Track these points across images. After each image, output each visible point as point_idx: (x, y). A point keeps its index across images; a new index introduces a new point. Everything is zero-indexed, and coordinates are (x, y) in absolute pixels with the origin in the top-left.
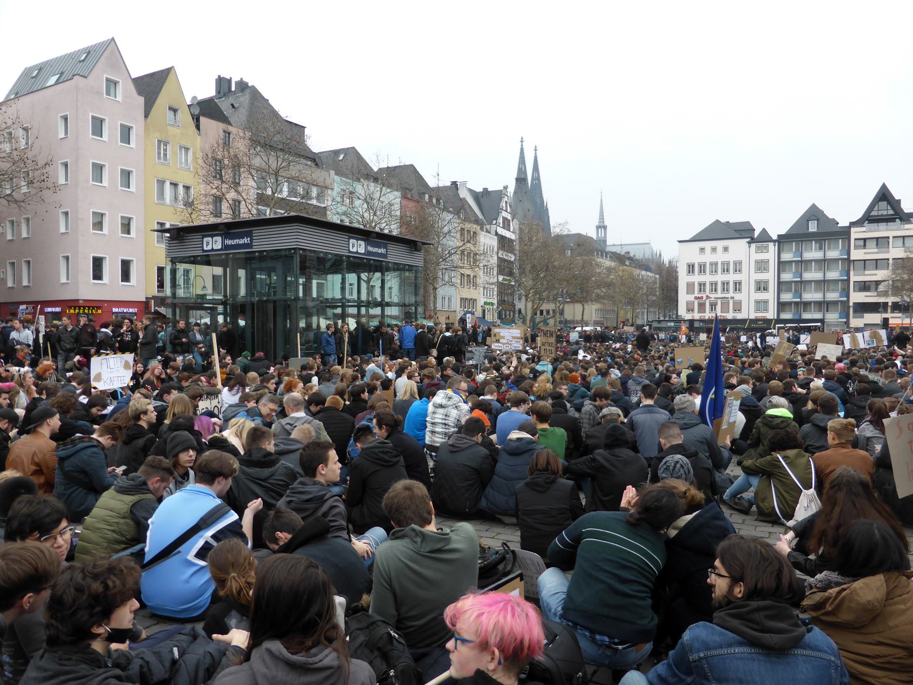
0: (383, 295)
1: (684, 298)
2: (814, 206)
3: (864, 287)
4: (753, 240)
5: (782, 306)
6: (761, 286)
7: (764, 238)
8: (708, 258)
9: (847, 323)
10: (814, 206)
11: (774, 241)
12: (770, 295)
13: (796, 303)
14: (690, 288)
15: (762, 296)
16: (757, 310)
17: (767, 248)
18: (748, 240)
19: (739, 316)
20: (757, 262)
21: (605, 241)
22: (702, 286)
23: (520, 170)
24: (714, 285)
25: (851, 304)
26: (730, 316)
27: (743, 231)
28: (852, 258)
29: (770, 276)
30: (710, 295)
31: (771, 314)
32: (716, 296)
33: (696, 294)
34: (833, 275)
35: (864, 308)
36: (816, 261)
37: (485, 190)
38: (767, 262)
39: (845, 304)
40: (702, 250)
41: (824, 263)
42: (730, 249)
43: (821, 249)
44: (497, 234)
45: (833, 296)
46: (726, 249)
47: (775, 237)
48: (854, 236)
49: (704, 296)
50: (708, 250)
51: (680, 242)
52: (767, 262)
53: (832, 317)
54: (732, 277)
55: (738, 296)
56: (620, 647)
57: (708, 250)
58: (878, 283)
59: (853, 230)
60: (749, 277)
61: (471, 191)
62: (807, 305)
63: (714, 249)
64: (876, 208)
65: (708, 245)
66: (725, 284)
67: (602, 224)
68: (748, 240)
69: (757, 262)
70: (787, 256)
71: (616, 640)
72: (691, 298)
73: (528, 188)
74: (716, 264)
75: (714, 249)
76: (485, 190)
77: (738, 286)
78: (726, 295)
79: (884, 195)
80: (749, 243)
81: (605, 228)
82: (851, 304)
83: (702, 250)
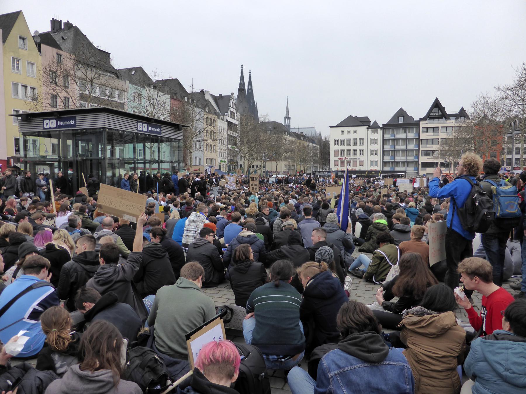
0: (159, 157)
1: (333, 159)
2: (401, 109)
3: (427, 153)
4: (369, 127)
5: (385, 163)
7: (375, 126)
8: (346, 136)
9: (418, 173)
10: (401, 109)
11: (381, 128)
12: (378, 158)
13: (392, 162)
14: (336, 152)
15: (374, 158)
16: (372, 166)
17: (377, 131)
19: (362, 169)
20: (372, 139)
21: (289, 126)
22: (343, 152)
23: (241, 84)
24: (349, 151)
25: (420, 163)
26: (357, 169)
27: (364, 122)
29: (378, 147)
31: (379, 168)
32: (350, 158)
34: (411, 147)
35: (426, 165)
36: (402, 139)
37: (220, 95)
38: (377, 139)
39: (417, 163)
40: (343, 132)
41: (406, 140)
42: (357, 132)
43: (405, 132)
44: (227, 121)
45: (411, 158)
46: (355, 132)
47: (381, 126)
50: (346, 132)
51: (331, 127)
52: (377, 139)
54: (358, 147)
55: (361, 158)
56: (283, 360)
57: (346, 132)
58: (433, 152)
59: (421, 122)
60: (367, 147)
61: (212, 96)
62: (397, 163)
63: (349, 132)
64: (433, 111)
65: (346, 129)
66: (355, 151)
67: (287, 116)
69: (372, 139)
70: (387, 136)
71: (281, 356)
72: (337, 158)
73: (246, 94)
74: (350, 140)
75: (349, 132)
76: (220, 95)
77: (361, 152)
78: (355, 157)
79: (437, 104)
80: (368, 129)
81: (289, 118)
82: (420, 163)
83: (343, 132)
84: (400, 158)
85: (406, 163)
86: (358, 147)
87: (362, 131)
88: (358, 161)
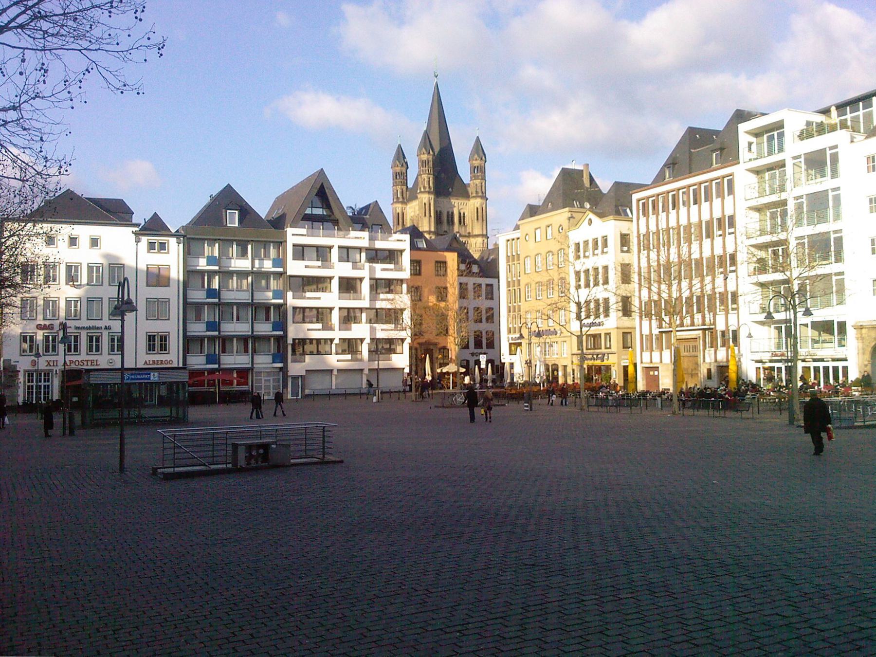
5: (189, 343)
9: (284, 370)
12: (171, 327)
16: (151, 348)
17: (163, 246)
33: (40, 321)
39: (281, 341)
46: (95, 242)
53: (263, 361)
57: (84, 241)
63: (73, 241)
75: (73, 241)
80: (136, 234)
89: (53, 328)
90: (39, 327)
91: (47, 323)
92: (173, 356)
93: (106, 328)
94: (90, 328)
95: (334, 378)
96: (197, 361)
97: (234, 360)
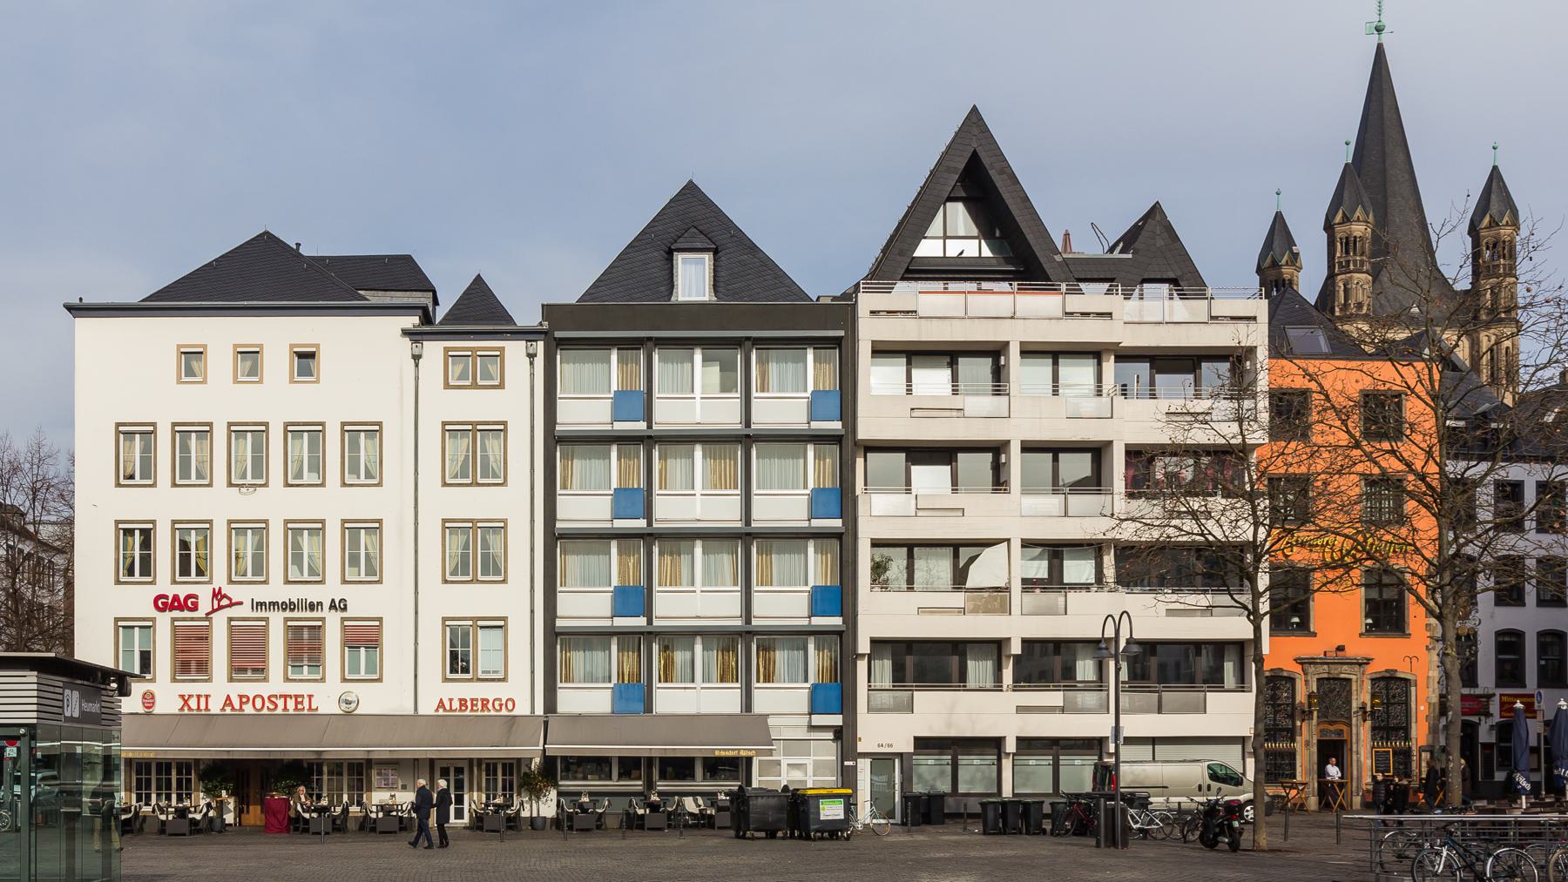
0: (1430, 370)
2: (691, 190)
6: (474, 552)
7: (480, 313)
8: (220, 400)
10: (691, 190)
11: (527, 334)
18: (412, 321)
19: (374, 700)
20: (450, 430)
25: (864, 647)
28: (865, 432)
29: (512, 503)
30: (234, 592)
40: (191, 360)
42: (324, 362)
46: (306, 358)
47: (527, 316)
48: (869, 330)
49: (204, 594)
50: (220, 363)
54: (334, 503)
55: (363, 601)
59: (866, 302)
60: (412, 502)
63: (250, 357)
64: (936, 227)
65: (220, 334)
68: (412, 321)
70: (585, 410)
72: (137, 600)
74: (149, 434)
75: (250, 357)
82: (864, 647)
84: (696, 597)
85: (743, 647)
86: (334, 503)
87: (365, 355)
88: (333, 622)
89: (195, 608)
90: (164, 604)
91: (183, 591)
92: (516, 688)
93: (333, 606)
94: (289, 606)
95: (1007, 764)
96: (587, 698)
97: (694, 698)
